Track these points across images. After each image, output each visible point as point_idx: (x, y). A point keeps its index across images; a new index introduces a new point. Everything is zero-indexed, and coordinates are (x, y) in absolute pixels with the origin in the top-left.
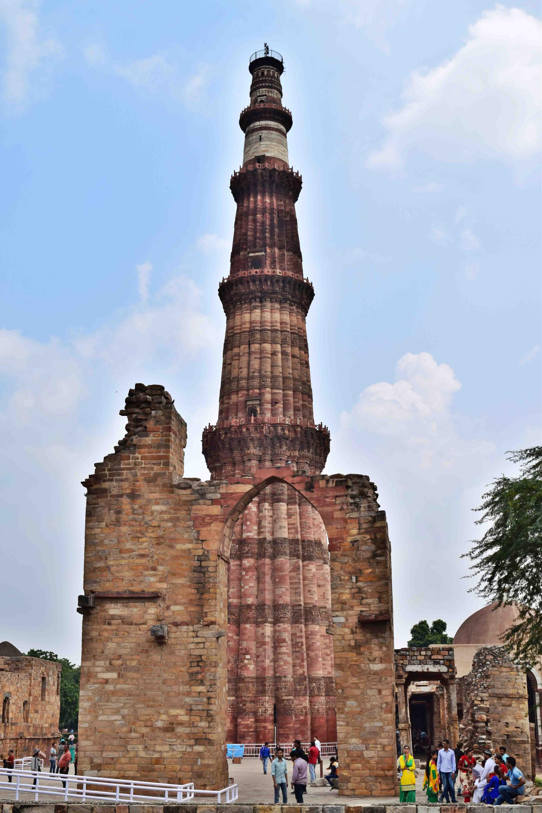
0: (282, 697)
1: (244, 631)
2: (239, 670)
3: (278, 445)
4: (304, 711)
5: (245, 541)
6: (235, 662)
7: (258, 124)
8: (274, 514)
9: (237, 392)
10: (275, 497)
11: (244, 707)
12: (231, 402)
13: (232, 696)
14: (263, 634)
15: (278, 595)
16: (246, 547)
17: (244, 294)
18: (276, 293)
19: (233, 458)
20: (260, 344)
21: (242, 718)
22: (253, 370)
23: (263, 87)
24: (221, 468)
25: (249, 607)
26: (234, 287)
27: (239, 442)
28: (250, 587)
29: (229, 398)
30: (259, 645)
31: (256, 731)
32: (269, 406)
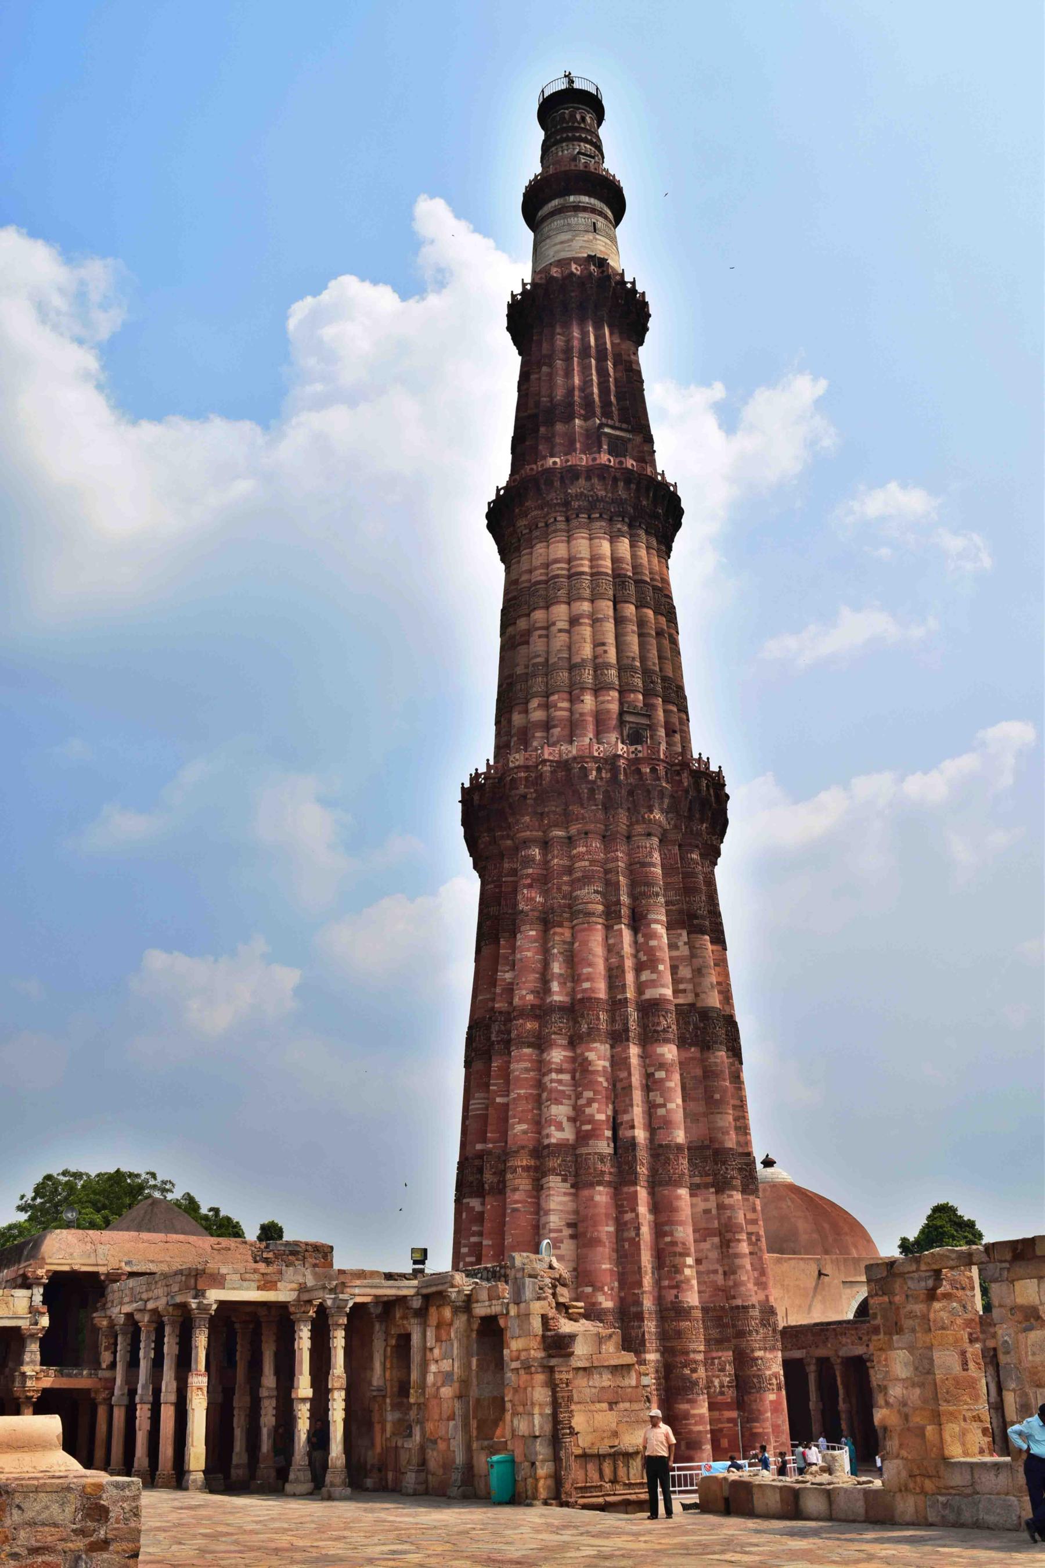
0: (753, 1351)
1: (676, 1203)
2: (674, 1292)
3: (697, 816)
4: (774, 1381)
5: (657, 1004)
6: (653, 1273)
7: (585, 199)
8: (693, 955)
9: (598, 690)
10: (695, 922)
11: (695, 1376)
12: (581, 708)
13: (656, 1351)
14: (707, 1212)
15: (722, 1128)
16: (661, 1018)
17: (602, 500)
18: (655, 516)
19: (606, 826)
20: (637, 607)
21: (689, 1401)
22: (632, 655)
23: (586, 141)
24: (570, 840)
25: (679, 1148)
26: (582, 481)
27: (631, 793)
28: (677, 1105)
29: (574, 699)
30: (697, 1235)
31: (712, 1431)
32: (662, 732)
